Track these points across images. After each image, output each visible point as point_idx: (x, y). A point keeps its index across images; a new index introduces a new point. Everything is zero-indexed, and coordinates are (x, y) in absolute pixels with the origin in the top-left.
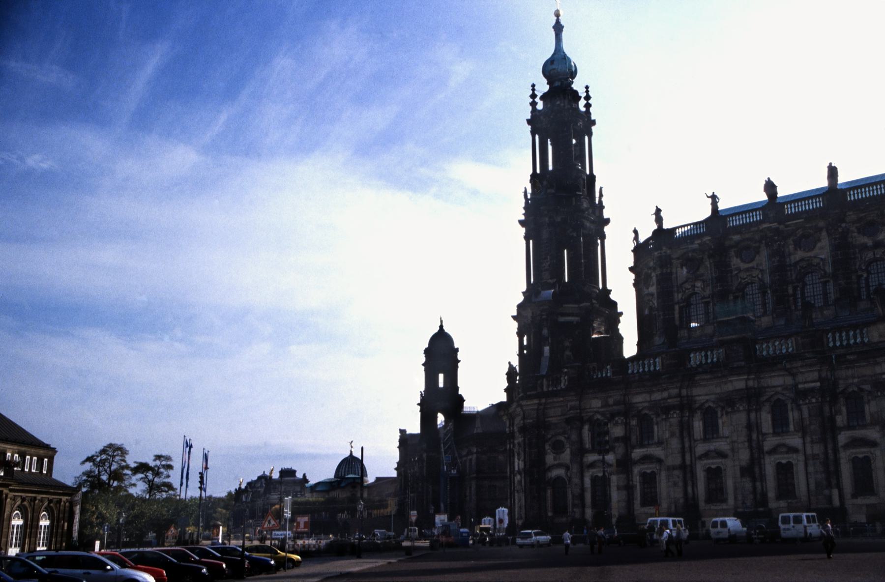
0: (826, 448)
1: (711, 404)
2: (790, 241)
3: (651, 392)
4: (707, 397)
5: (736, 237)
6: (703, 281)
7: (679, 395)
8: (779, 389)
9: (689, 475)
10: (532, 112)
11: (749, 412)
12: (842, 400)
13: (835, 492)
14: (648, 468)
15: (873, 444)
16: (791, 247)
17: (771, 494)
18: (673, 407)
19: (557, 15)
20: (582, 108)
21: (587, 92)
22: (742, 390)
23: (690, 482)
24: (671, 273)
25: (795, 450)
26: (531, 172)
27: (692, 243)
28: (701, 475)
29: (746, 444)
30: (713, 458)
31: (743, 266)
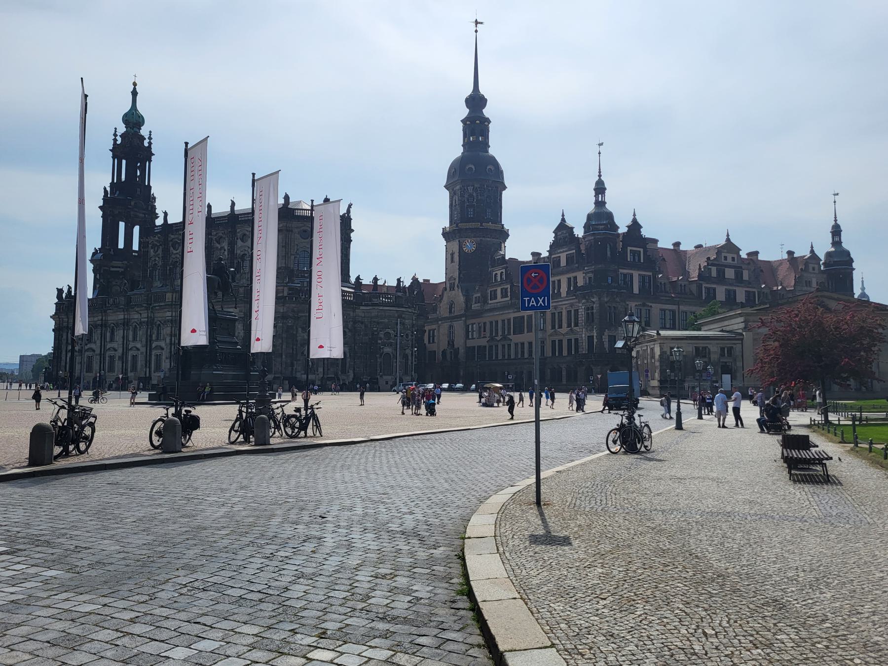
0: (147, 349)
5: (172, 236)
6: (159, 258)
7: (102, 320)
8: (136, 320)
9: (102, 359)
12: (155, 328)
13: (148, 369)
14: (90, 354)
15: (163, 349)
17: (129, 370)
19: (135, 84)
20: (146, 144)
21: (150, 135)
24: (148, 251)
25: (138, 349)
31: (175, 252)
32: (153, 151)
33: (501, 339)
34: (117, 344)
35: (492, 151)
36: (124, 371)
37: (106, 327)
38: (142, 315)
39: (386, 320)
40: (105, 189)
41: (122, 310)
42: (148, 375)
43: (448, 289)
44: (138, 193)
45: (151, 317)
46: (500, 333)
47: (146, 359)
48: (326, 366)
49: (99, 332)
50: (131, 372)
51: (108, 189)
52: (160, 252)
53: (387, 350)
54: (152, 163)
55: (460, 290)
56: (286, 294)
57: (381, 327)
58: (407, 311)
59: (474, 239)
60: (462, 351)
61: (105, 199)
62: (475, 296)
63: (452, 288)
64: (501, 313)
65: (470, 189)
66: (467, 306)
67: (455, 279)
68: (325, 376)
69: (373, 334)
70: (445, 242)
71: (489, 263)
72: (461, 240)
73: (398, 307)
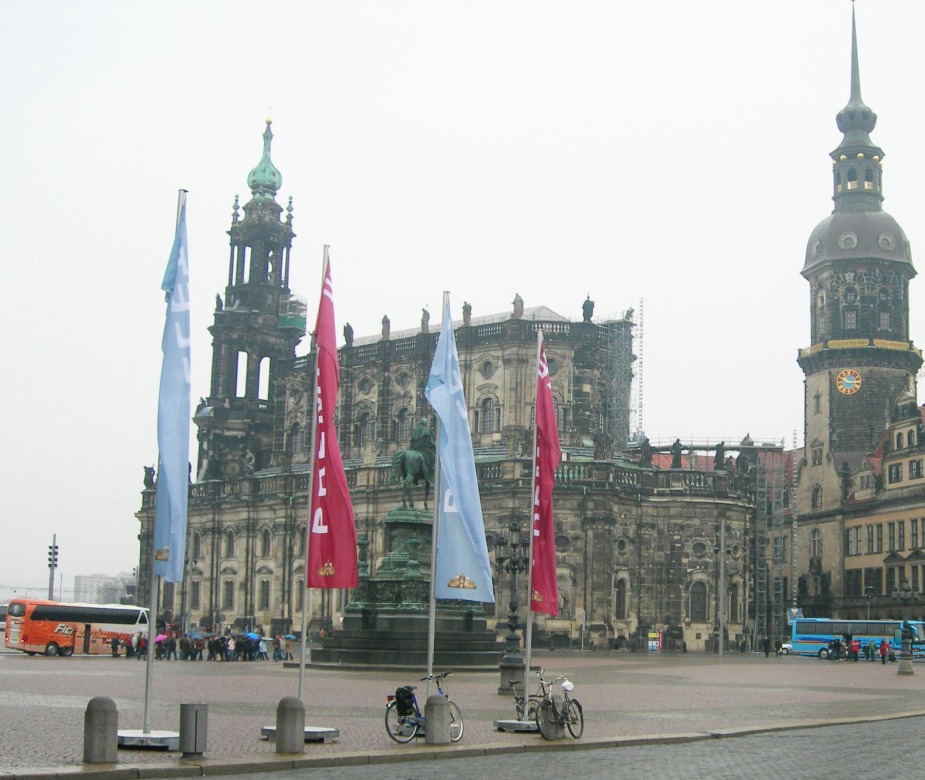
1: (231, 529)
2: (356, 384)
3: (200, 515)
4: (230, 524)
6: (302, 413)
7: (213, 520)
8: (267, 521)
10: (233, 224)
11: (248, 538)
12: (298, 535)
13: (286, 606)
16: (357, 389)
18: (209, 529)
20: (283, 218)
21: (290, 203)
22: (245, 519)
23: (214, 593)
24: (284, 402)
25: (271, 572)
26: (227, 284)
27: (296, 377)
28: (222, 586)
29: (244, 564)
30: (227, 574)
32: (294, 230)
33: (909, 558)
34: (237, 563)
35: (888, 207)
36: (248, 607)
37: (219, 532)
38: (277, 512)
39: (696, 522)
40: (218, 298)
41: (245, 504)
42: (286, 616)
43: (810, 462)
44: (269, 301)
45: (291, 516)
46: (908, 544)
47: (283, 588)
48: (589, 605)
49: (209, 541)
50: (260, 609)
51: (223, 298)
52: (304, 402)
53: (699, 576)
54: (292, 250)
55: (832, 465)
56: (517, 475)
57: (689, 534)
58: (736, 505)
59: (859, 369)
60: (836, 578)
61: (218, 317)
62: (862, 474)
63: (817, 461)
64: (910, 506)
65: (849, 277)
66: (845, 494)
67: (822, 444)
68: (589, 624)
69: (673, 548)
70: (803, 376)
71: (887, 412)
72: (834, 370)
73: (719, 497)
